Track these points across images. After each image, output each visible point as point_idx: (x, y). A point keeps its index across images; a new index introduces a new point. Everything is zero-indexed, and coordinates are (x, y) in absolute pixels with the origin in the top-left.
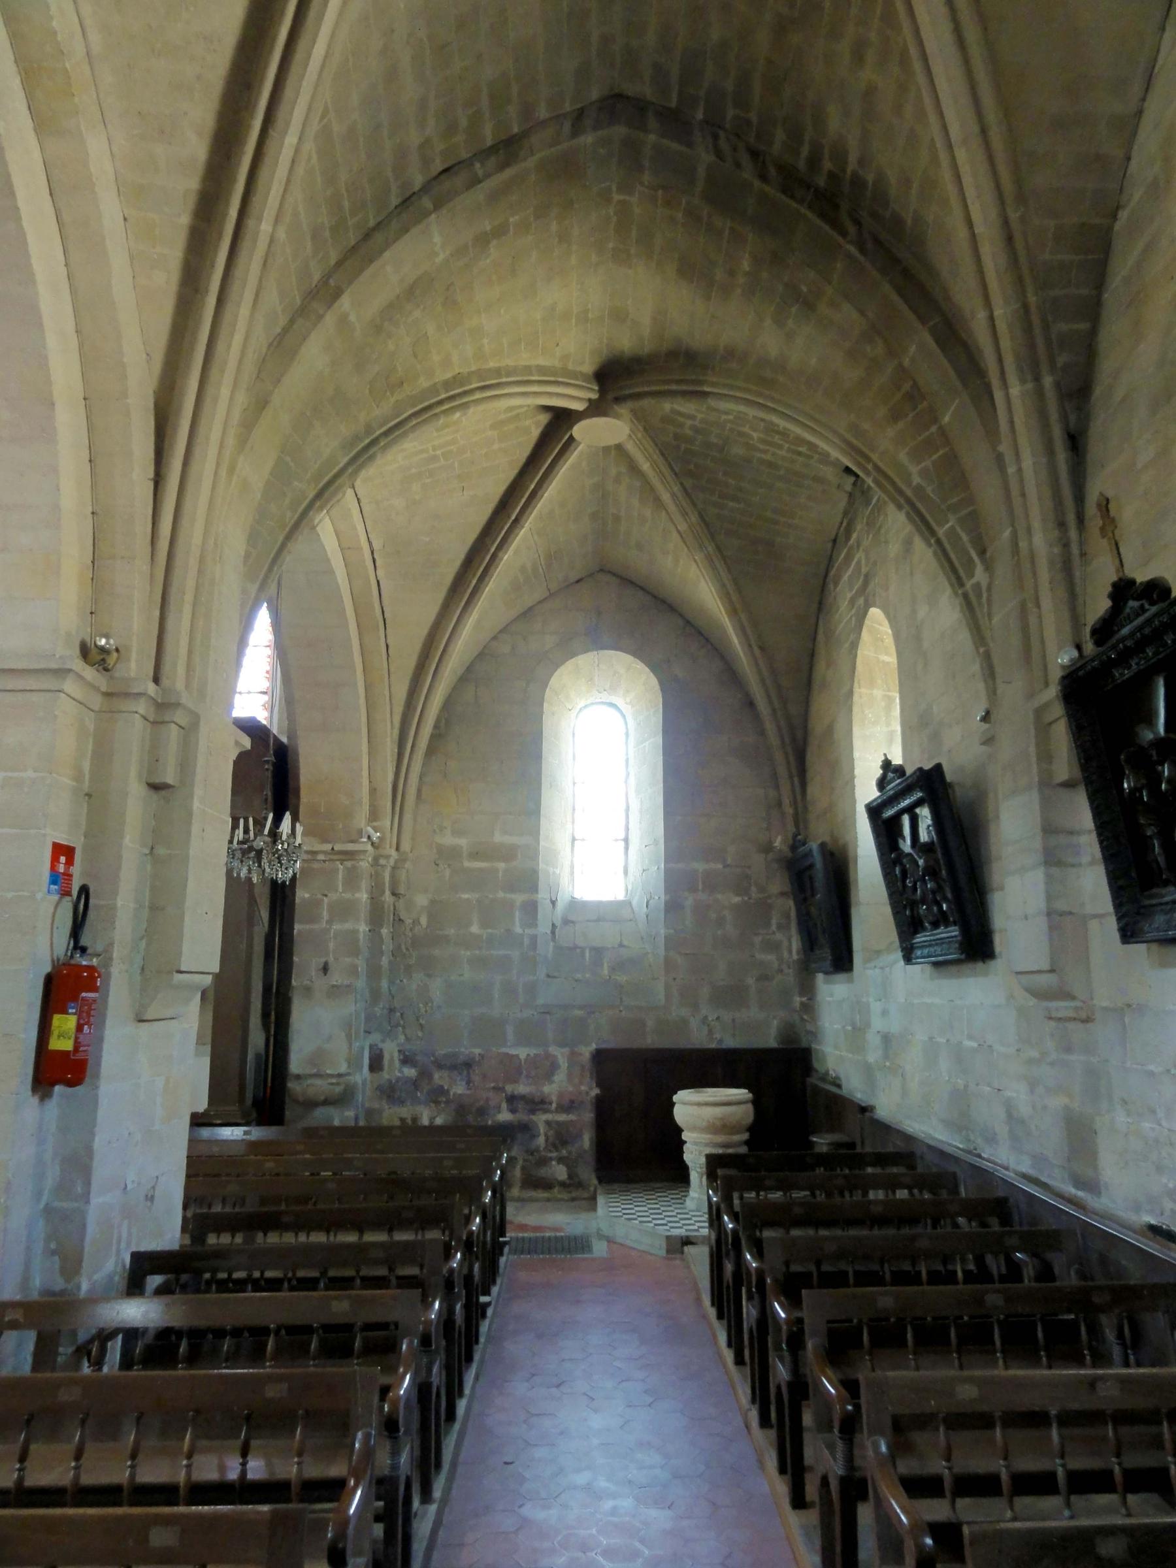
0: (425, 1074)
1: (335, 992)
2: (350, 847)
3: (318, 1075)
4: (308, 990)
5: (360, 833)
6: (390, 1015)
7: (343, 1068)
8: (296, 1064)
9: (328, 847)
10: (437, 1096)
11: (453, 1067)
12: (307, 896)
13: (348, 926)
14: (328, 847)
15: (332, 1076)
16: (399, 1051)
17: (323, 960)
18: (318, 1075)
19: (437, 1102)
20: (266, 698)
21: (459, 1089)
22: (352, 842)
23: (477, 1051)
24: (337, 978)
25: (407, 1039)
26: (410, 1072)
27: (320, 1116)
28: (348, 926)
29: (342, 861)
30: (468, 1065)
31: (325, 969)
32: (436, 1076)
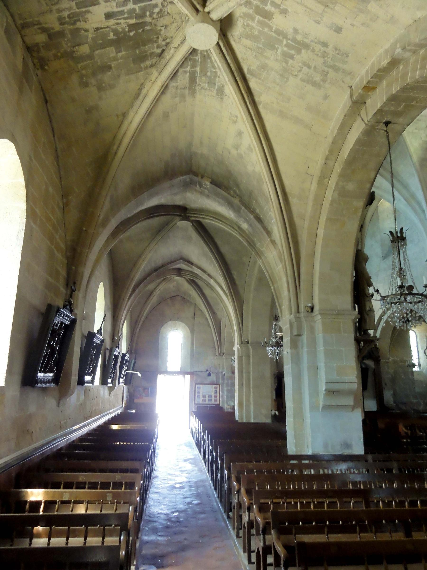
4: (385, 388)
31: (386, 384)
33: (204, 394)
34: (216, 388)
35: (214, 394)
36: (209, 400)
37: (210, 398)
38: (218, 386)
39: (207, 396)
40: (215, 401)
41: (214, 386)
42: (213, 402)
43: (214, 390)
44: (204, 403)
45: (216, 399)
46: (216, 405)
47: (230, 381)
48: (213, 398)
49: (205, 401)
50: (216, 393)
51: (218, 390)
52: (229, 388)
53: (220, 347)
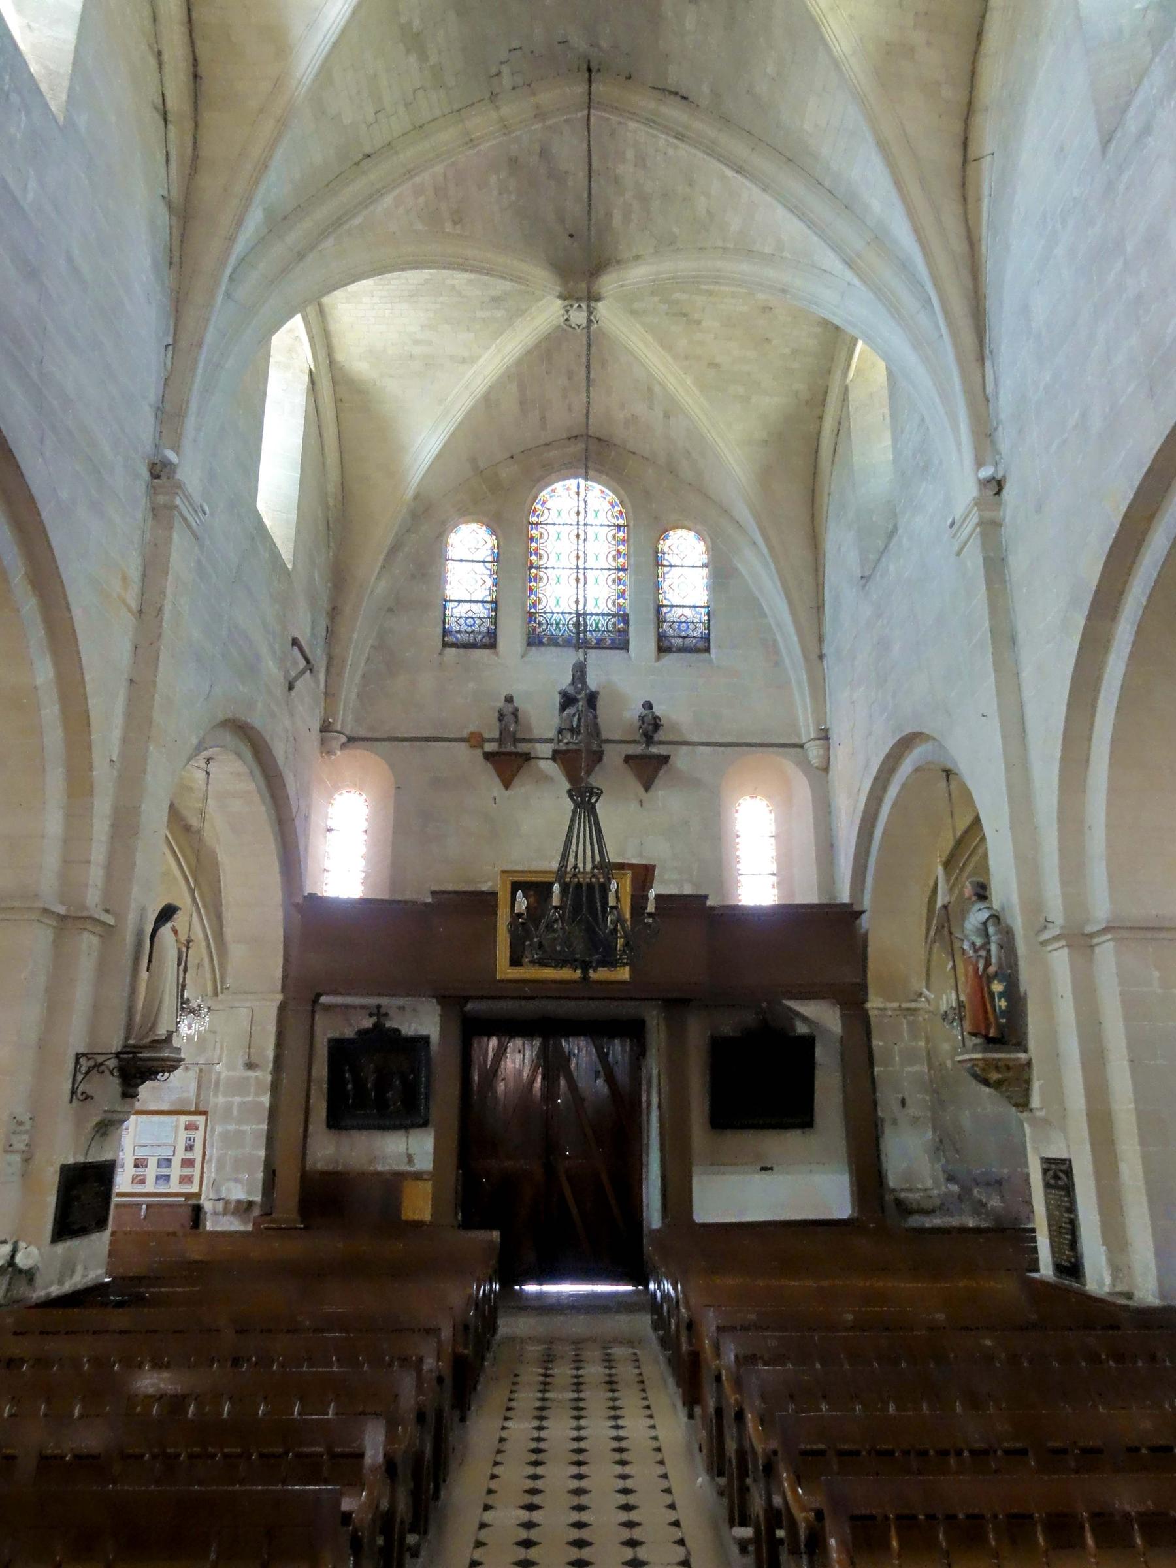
0: (966, 1191)
1: (915, 1120)
2: (913, 1005)
3: (910, 1190)
4: (895, 1122)
5: (920, 995)
6: (945, 1143)
7: (929, 1183)
8: (892, 1181)
9: (895, 1005)
10: (979, 1207)
11: (988, 1184)
12: (881, 1044)
13: (917, 1068)
14: (895, 1005)
15: (919, 1190)
16: (944, 1172)
17: (900, 1096)
18: (910, 1190)
19: (979, 1214)
20: (774, 879)
21: (995, 1203)
22: (916, 1001)
23: (1006, 1171)
24: (912, 1110)
25: (947, 1161)
26: (954, 1188)
27: (915, 1221)
28: (917, 1068)
29: (905, 1016)
30: (999, 1182)
31: (903, 1103)
32: (975, 1191)
33: (141, 1153)
34: (190, 1127)
35: (181, 1154)
36: (158, 1177)
37: (165, 1171)
38: (200, 1120)
39: (152, 1162)
40: (185, 1180)
41: (184, 1119)
42: (174, 1186)
43: (183, 1135)
44: (139, 1189)
45: (187, 1171)
46: (188, 1196)
47: (237, 1099)
48: (176, 1171)
49: (143, 1182)
50: (189, 1148)
51: (199, 1136)
52: (232, 1127)
53: (221, 965)
